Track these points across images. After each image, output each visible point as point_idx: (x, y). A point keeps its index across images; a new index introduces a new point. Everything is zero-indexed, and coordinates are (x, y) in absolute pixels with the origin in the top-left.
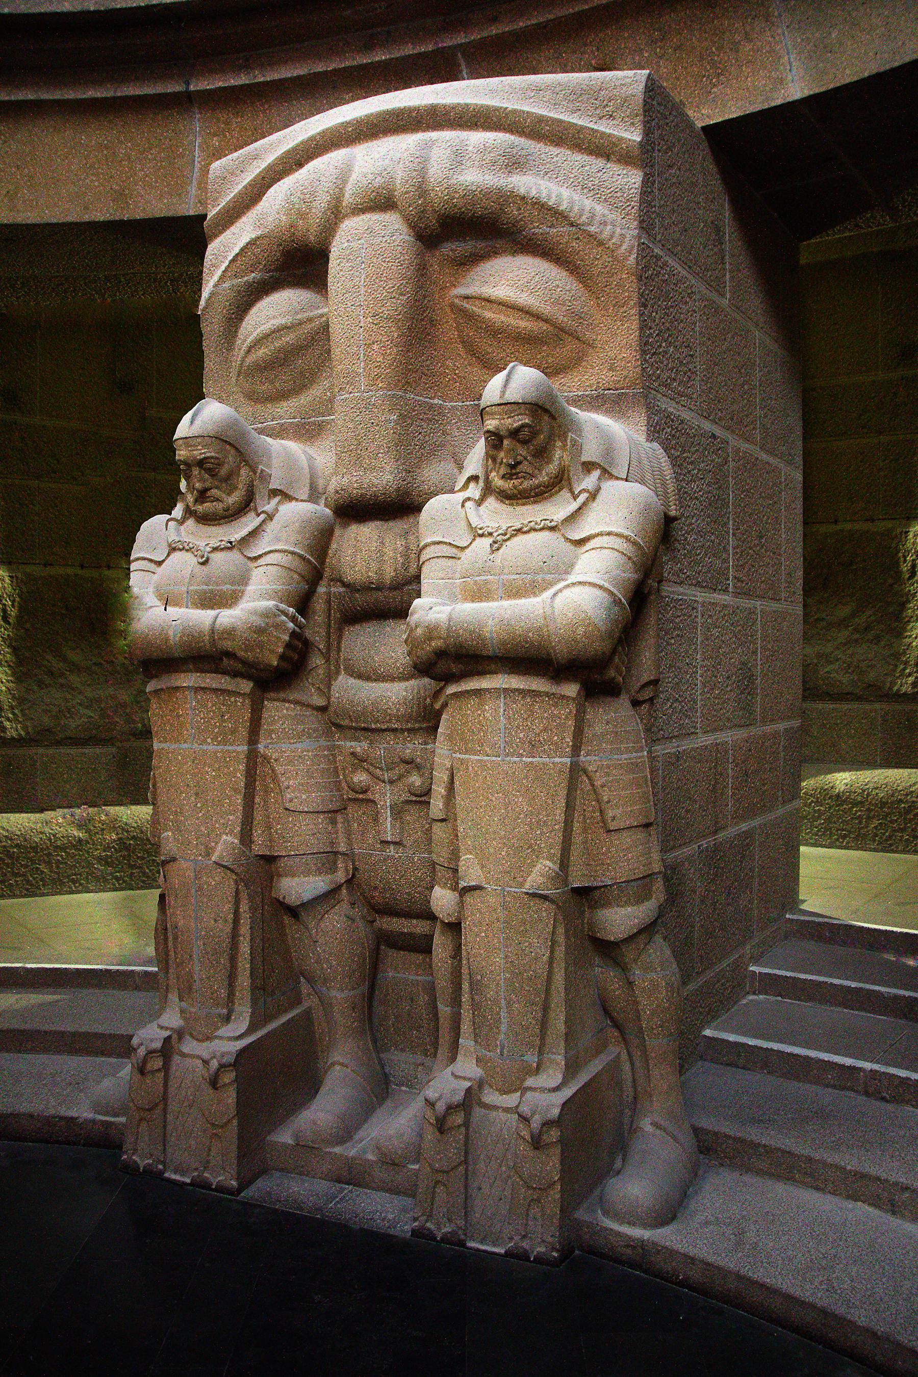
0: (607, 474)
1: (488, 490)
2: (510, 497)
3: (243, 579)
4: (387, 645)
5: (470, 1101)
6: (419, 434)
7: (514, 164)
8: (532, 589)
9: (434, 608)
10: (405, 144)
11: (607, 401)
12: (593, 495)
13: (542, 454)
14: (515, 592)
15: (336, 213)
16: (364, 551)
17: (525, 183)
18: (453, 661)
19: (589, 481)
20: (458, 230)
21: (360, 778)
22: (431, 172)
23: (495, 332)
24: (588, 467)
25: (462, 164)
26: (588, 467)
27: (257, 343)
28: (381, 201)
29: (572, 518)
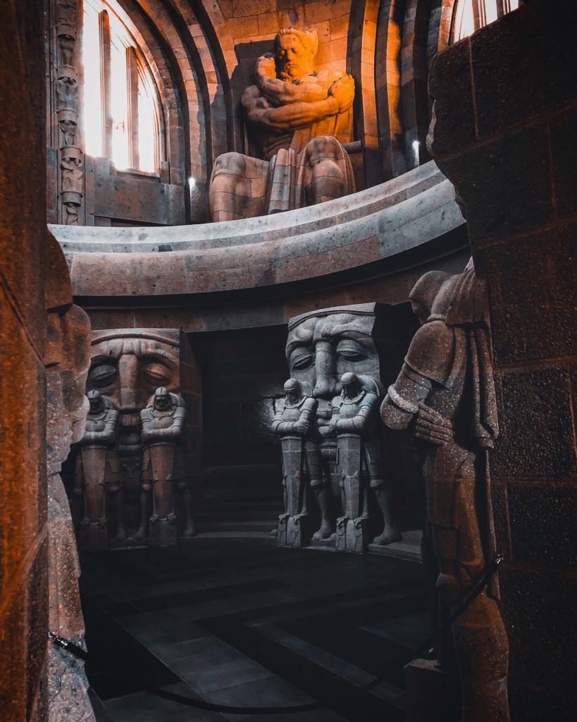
0: (177, 406)
1: (155, 408)
2: (161, 410)
3: (104, 426)
4: (133, 438)
5: (158, 520)
6: (141, 399)
7: (157, 347)
8: (167, 427)
9: (148, 430)
10: (136, 341)
11: (174, 391)
12: (175, 410)
13: (167, 403)
14: (164, 428)
15: (121, 354)
16: (128, 420)
17: (160, 351)
18: (155, 439)
19: (175, 407)
20: (144, 360)
21: (125, 465)
22: (142, 348)
23: (153, 378)
24: (174, 405)
25: (149, 346)
26: (174, 405)
27: (98, 376)
28: (131, 353)
29: (172, 415)
